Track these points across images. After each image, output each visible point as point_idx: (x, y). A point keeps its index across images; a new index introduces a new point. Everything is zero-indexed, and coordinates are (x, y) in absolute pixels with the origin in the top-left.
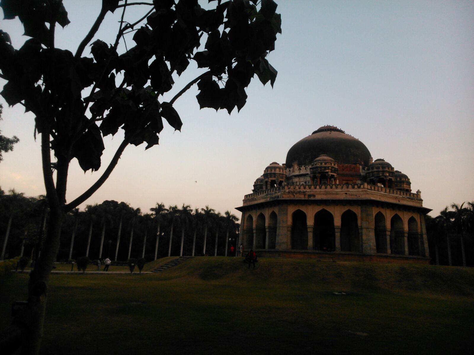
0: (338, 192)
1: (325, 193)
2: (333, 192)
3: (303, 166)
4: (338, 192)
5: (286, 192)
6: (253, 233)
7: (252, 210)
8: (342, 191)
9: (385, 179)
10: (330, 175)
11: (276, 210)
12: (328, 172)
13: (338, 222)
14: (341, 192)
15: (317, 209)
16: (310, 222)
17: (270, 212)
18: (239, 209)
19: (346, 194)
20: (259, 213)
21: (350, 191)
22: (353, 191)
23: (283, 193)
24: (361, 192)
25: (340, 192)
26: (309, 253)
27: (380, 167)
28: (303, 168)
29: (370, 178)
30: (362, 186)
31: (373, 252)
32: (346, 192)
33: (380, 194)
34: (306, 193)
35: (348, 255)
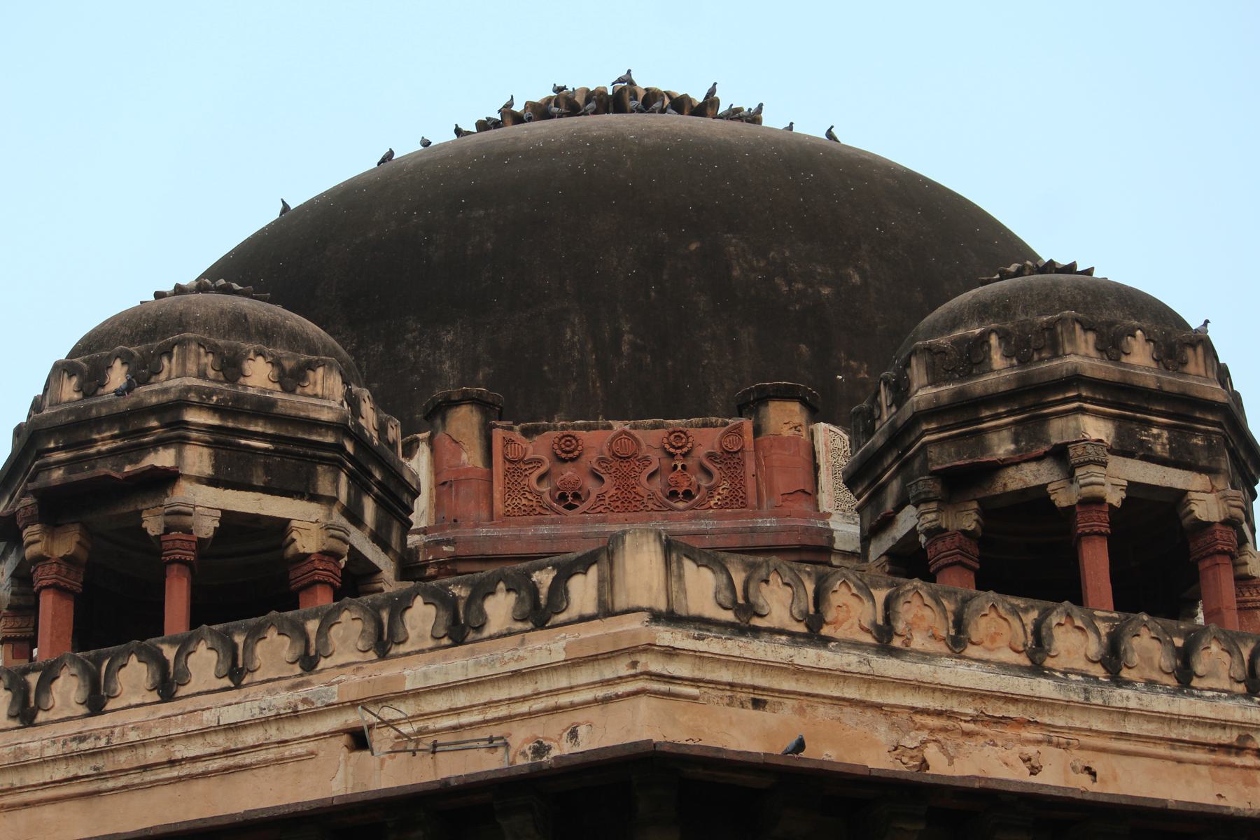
0: (250, 737)
1: (85, 769)
2: (180, 751)
4: (250, 737)
8: (295, 715)
9: (1062, 499)
12: (168, 478)
14: (291, 730)
21: (404, 696)
22: (467, 685)
24: (562, 681)
25: (274, 733)
27: (983, 339)
30: (583, 590)
32: (352, 718)
33: (917, 686)
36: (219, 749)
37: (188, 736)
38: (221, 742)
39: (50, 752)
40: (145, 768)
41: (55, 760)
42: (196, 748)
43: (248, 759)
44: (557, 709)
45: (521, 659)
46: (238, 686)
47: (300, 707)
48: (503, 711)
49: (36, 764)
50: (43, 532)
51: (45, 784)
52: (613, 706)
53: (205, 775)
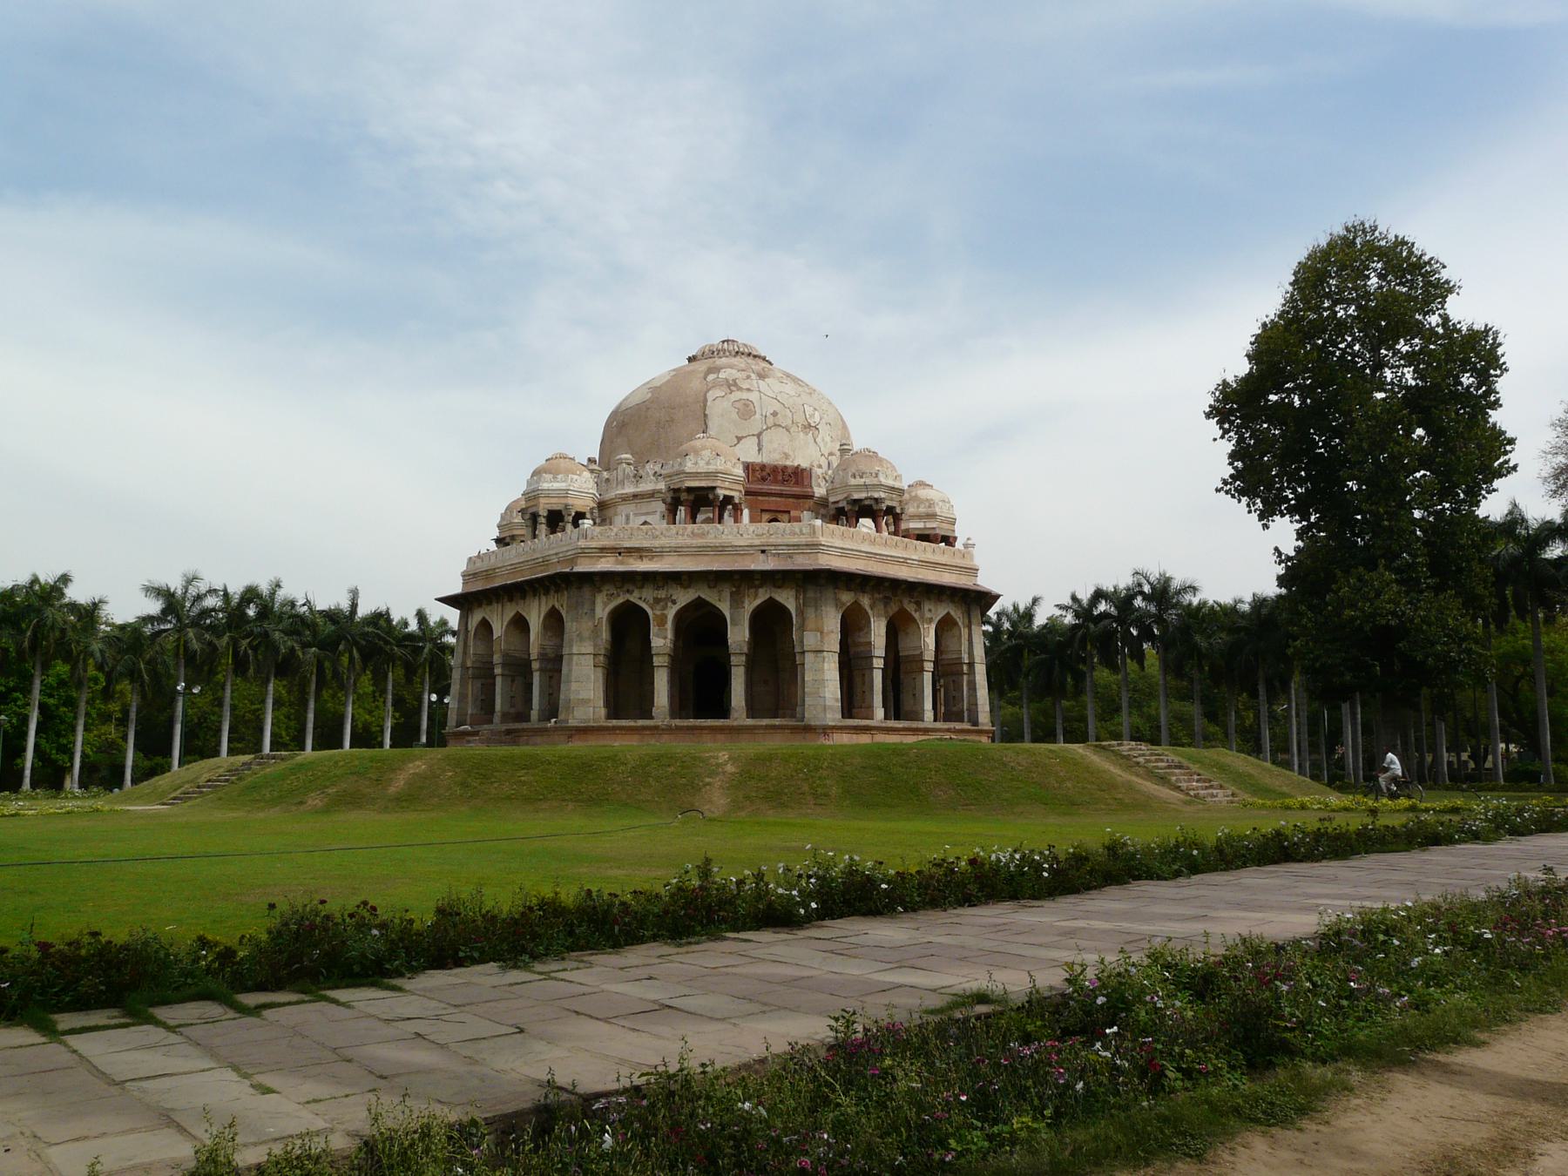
6: (494, 677)
7: (490, 603)
9: (875, 507)
10: (721, 498)
11: (561, 602)
13: (739, 635)
15: (684, 597)
16: (661, 641)
17: (544, 610)
18: (449, 601)
19: (763, 552)
20: (510, 613)
26: (656, 728)
29: (836, 506)
31: (833, 717)
32: (763, 548)
35: (767, 727)
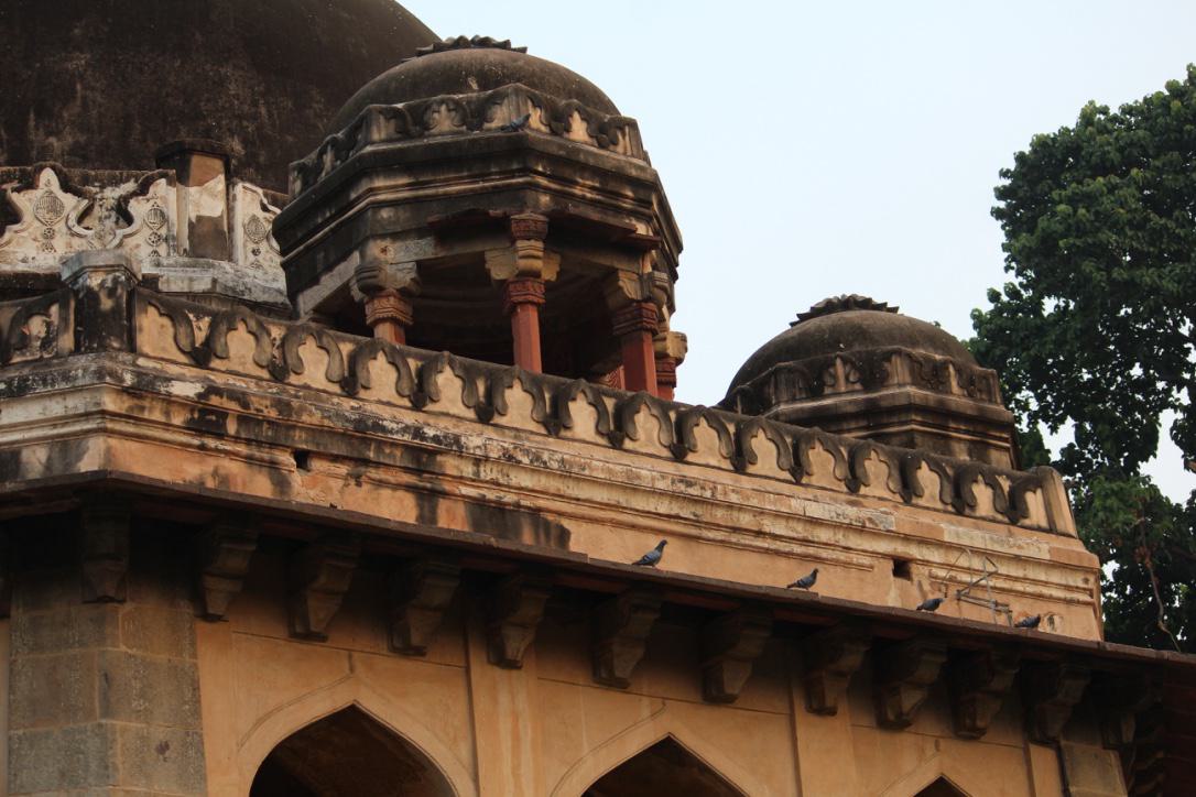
0: (824, 535)
1: (686, 511)
2: (769, 526)
3: (48, 177)
4: (824, 535)
5: (169, 401)
8: (861, 530)
14: (854, 541)
23: (110, 403)
25: (840, 537)
27: (944, 365)
28: (55, 207)
32: (901, 549)
34: (450, 464)
36: (800, 536)
37: (777, 515)
38: (800, 530)
39: (661, 485)
40: (735, 530)
41: (662, 494)
42: (779, 528)
43: (824, 553)
44: (1039, 597)
45: (1020, 547)
46: (798, 483)
47: (868, 524)
48: (1000, 584)
49: (645, 491)
50: (545, 250)
51: (649, 512)
52: (1073, 608)
53: (788, 555)
